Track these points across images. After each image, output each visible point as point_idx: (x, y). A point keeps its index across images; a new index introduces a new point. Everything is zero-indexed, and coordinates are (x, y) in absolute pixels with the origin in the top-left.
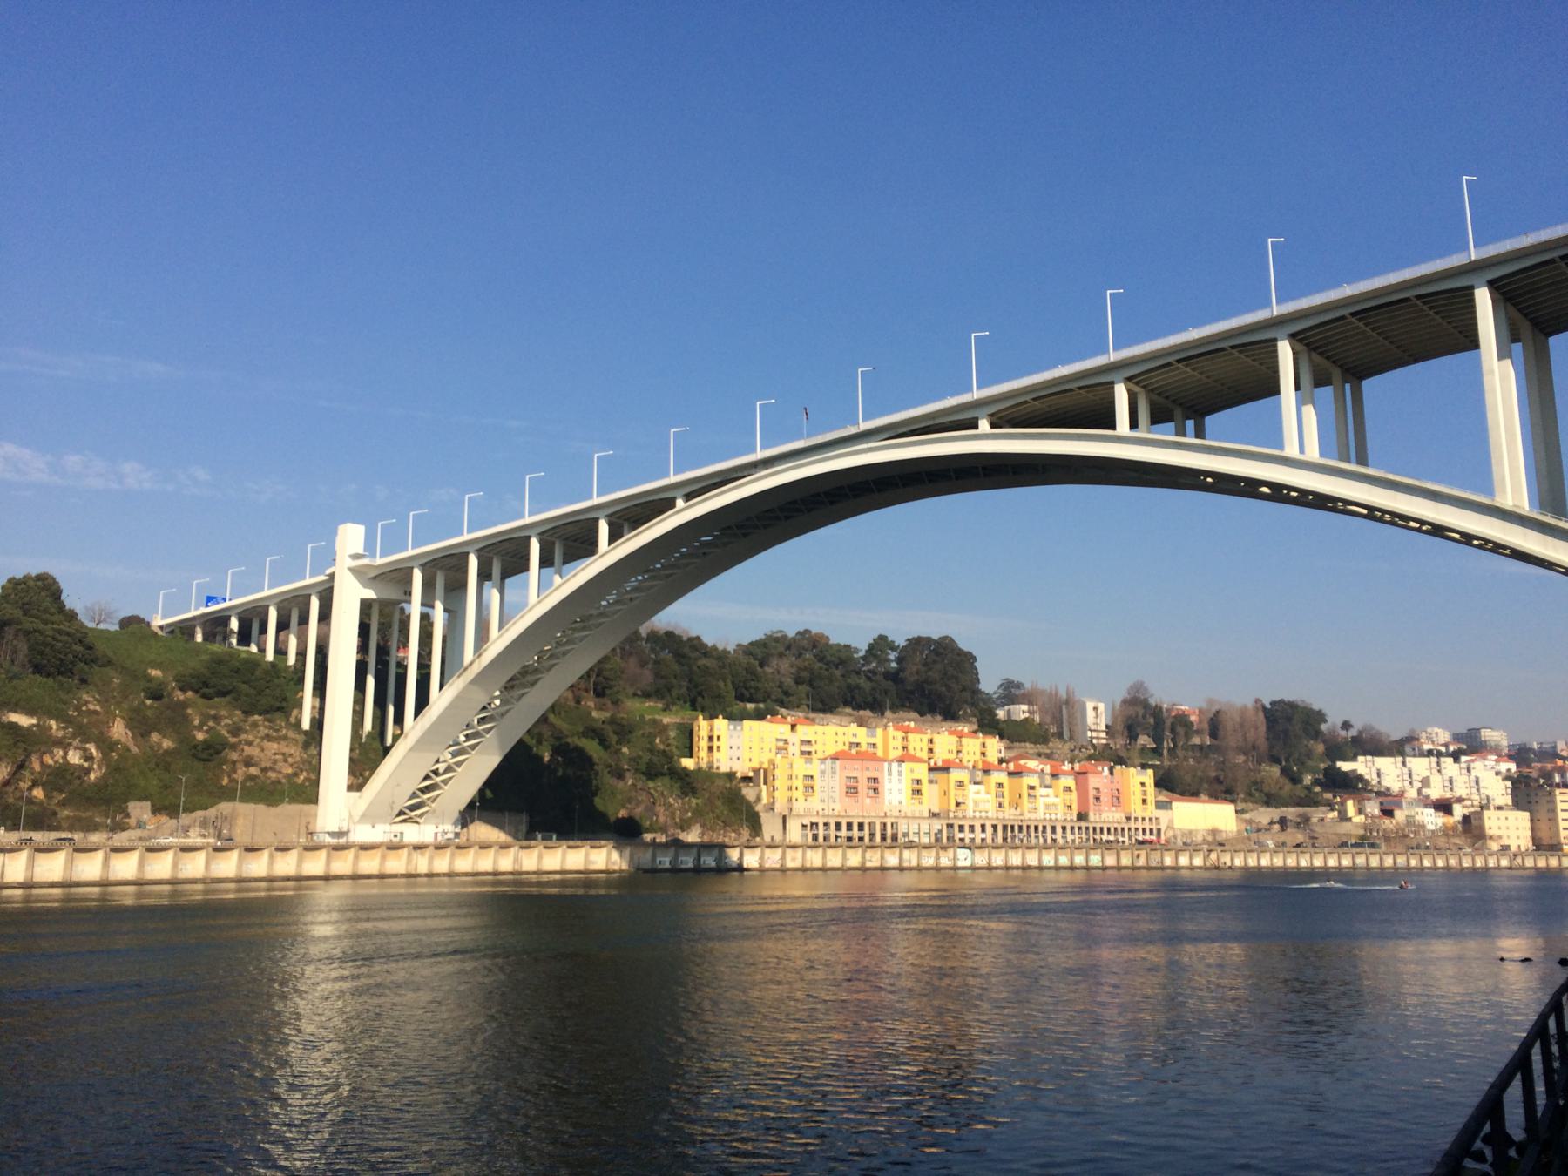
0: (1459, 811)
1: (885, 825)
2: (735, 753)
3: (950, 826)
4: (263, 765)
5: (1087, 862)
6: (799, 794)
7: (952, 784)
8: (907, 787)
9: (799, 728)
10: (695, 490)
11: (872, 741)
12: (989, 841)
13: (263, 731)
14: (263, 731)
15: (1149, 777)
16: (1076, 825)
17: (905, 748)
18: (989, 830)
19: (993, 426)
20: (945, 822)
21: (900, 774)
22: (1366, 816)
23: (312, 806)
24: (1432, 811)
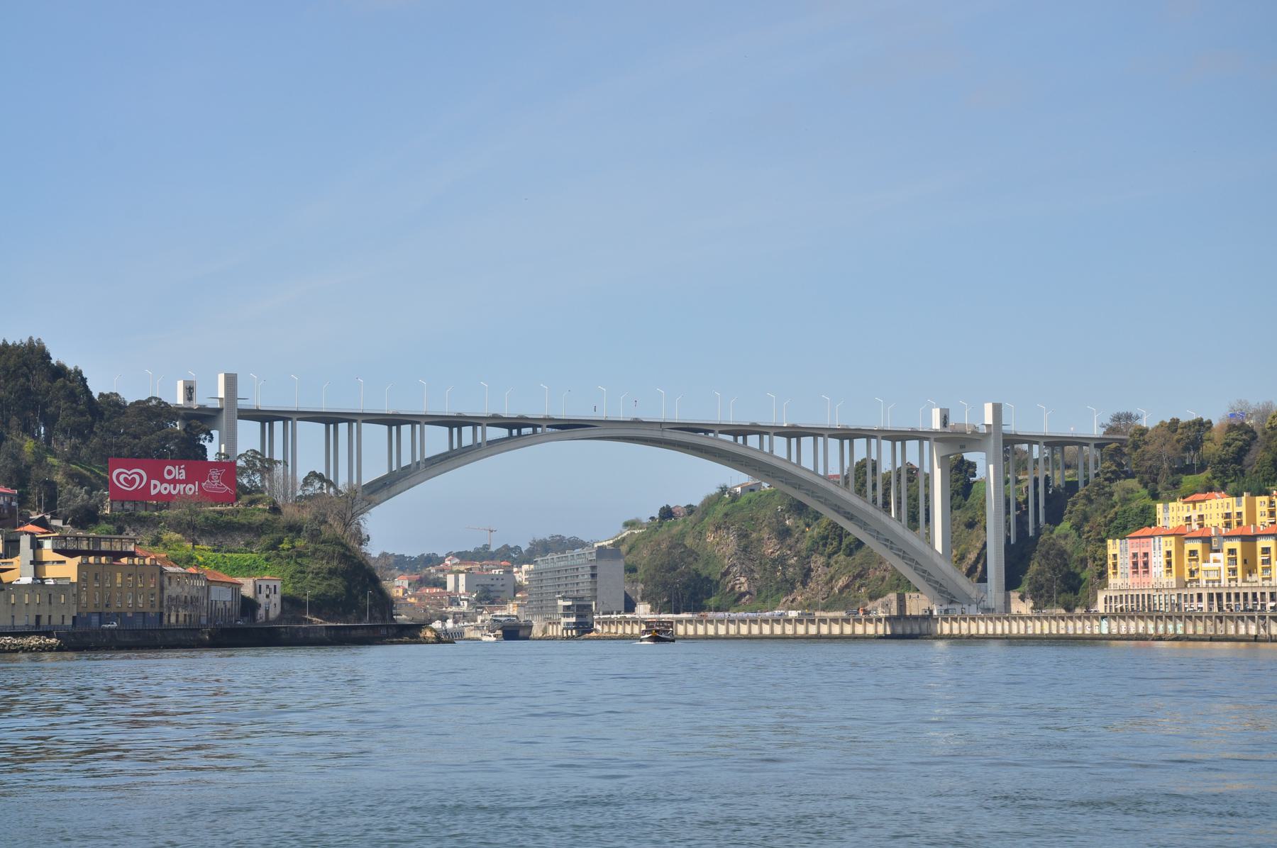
1: (1143, 595)
5: (1226, 631)
7: (1186, 552)
8: (1163, 560)
9: (1197, 505)
12: (1206, 609)
16: (1176, 592)
18: (1205, 598)
21: (1160, 549)
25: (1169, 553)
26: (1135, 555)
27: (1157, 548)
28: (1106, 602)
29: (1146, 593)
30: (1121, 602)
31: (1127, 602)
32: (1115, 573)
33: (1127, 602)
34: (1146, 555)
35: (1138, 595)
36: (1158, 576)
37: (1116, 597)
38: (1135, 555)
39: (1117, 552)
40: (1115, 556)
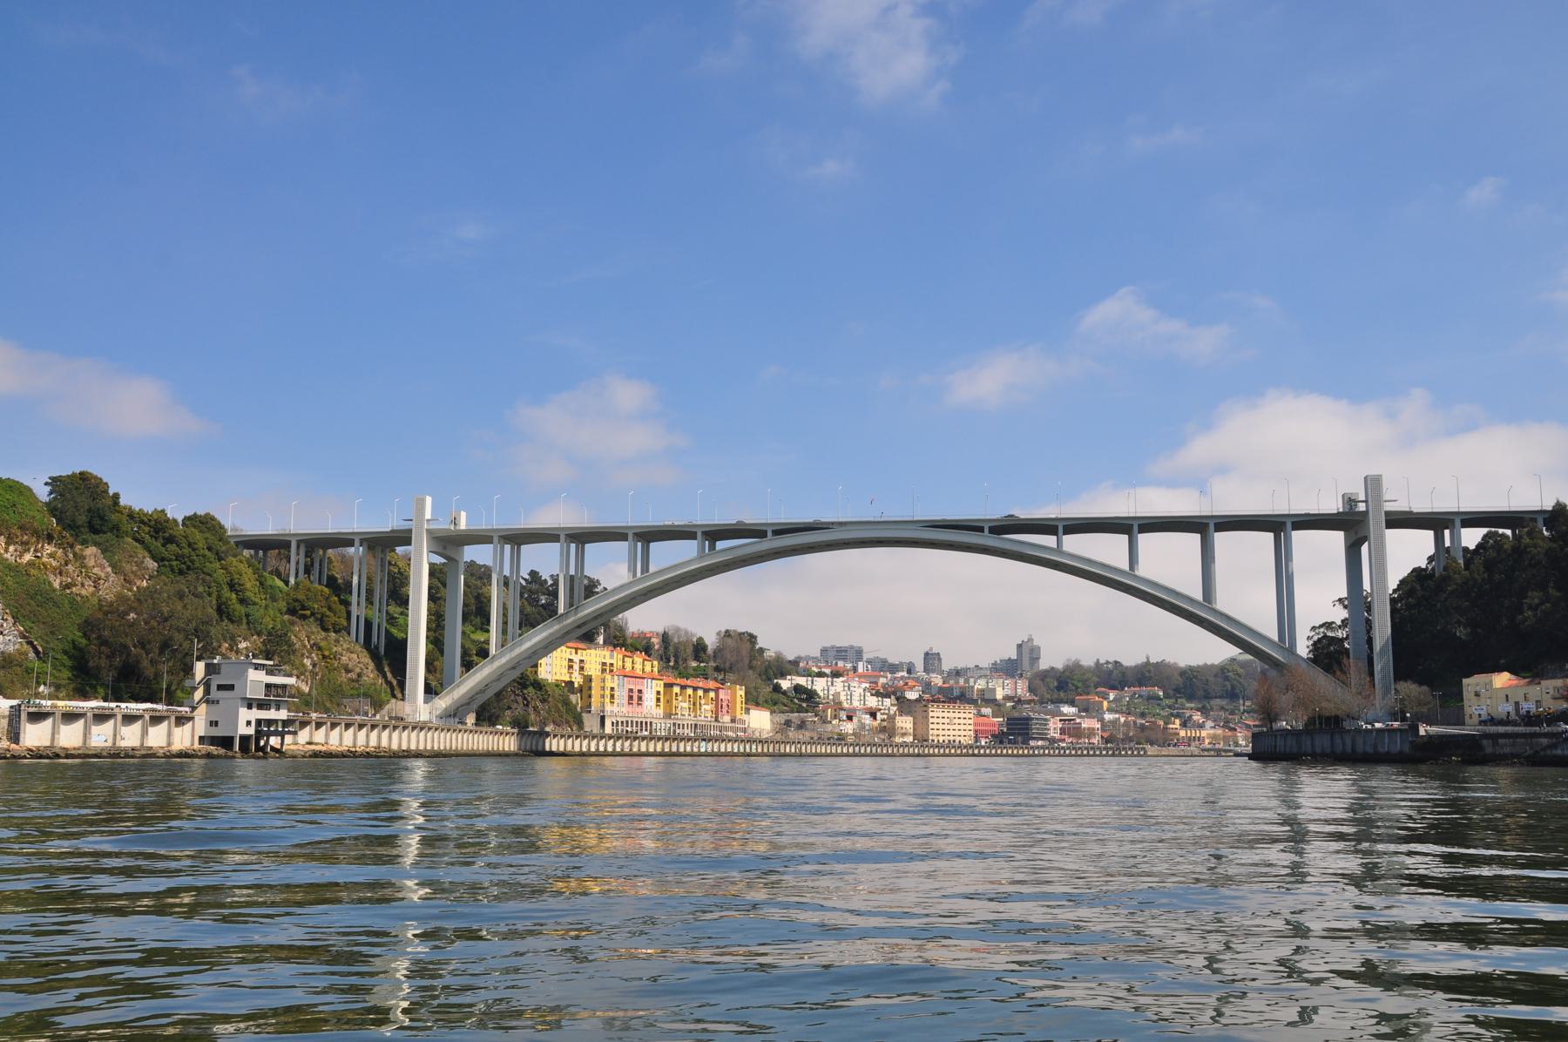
0: (879, 716)
1: (646, 723)
2: (549, 668)
3: (674, 724)
4: (358, 670)
6: (607, 700)
8: (654, 696)
9: (579, 651)
10: (781, 531)
11: (612, 662)
13: (345, 646)
14: (345, 646)
15: (741, 692)
17: (633, 668)
19: (990, 533)
20: (672, 722)
22: (840, 720)
23: (400, 703)
24: (868, 716)
25: (658, 693)
26: (631, 690)
27: (649, 687)
28: (613, 725)
29: (649, 721)
30: (627, 726)
31: (632, 726)
32: (612, 703)
33: (632, 726)
34: (640, 691)
35: (637, 722)
36: (649, 708)
37: (622, 722)
38: (631, 690)
39: (615, 685)
40: (612, 689)
